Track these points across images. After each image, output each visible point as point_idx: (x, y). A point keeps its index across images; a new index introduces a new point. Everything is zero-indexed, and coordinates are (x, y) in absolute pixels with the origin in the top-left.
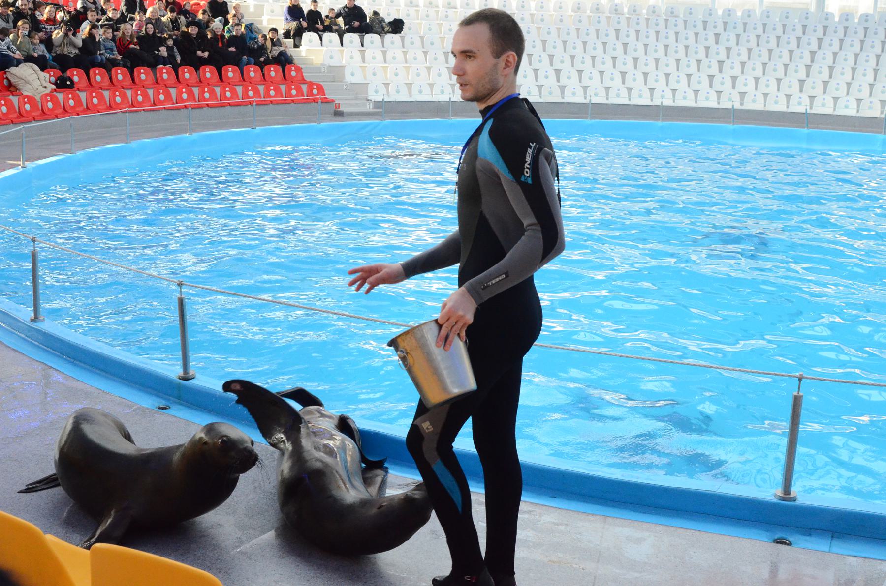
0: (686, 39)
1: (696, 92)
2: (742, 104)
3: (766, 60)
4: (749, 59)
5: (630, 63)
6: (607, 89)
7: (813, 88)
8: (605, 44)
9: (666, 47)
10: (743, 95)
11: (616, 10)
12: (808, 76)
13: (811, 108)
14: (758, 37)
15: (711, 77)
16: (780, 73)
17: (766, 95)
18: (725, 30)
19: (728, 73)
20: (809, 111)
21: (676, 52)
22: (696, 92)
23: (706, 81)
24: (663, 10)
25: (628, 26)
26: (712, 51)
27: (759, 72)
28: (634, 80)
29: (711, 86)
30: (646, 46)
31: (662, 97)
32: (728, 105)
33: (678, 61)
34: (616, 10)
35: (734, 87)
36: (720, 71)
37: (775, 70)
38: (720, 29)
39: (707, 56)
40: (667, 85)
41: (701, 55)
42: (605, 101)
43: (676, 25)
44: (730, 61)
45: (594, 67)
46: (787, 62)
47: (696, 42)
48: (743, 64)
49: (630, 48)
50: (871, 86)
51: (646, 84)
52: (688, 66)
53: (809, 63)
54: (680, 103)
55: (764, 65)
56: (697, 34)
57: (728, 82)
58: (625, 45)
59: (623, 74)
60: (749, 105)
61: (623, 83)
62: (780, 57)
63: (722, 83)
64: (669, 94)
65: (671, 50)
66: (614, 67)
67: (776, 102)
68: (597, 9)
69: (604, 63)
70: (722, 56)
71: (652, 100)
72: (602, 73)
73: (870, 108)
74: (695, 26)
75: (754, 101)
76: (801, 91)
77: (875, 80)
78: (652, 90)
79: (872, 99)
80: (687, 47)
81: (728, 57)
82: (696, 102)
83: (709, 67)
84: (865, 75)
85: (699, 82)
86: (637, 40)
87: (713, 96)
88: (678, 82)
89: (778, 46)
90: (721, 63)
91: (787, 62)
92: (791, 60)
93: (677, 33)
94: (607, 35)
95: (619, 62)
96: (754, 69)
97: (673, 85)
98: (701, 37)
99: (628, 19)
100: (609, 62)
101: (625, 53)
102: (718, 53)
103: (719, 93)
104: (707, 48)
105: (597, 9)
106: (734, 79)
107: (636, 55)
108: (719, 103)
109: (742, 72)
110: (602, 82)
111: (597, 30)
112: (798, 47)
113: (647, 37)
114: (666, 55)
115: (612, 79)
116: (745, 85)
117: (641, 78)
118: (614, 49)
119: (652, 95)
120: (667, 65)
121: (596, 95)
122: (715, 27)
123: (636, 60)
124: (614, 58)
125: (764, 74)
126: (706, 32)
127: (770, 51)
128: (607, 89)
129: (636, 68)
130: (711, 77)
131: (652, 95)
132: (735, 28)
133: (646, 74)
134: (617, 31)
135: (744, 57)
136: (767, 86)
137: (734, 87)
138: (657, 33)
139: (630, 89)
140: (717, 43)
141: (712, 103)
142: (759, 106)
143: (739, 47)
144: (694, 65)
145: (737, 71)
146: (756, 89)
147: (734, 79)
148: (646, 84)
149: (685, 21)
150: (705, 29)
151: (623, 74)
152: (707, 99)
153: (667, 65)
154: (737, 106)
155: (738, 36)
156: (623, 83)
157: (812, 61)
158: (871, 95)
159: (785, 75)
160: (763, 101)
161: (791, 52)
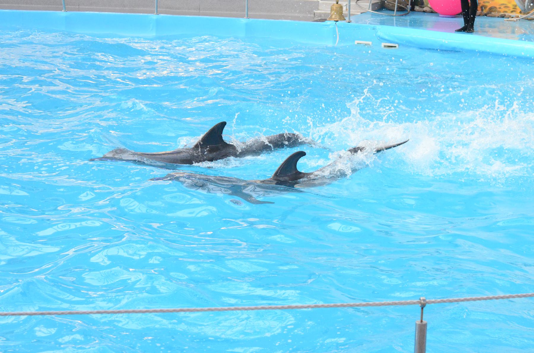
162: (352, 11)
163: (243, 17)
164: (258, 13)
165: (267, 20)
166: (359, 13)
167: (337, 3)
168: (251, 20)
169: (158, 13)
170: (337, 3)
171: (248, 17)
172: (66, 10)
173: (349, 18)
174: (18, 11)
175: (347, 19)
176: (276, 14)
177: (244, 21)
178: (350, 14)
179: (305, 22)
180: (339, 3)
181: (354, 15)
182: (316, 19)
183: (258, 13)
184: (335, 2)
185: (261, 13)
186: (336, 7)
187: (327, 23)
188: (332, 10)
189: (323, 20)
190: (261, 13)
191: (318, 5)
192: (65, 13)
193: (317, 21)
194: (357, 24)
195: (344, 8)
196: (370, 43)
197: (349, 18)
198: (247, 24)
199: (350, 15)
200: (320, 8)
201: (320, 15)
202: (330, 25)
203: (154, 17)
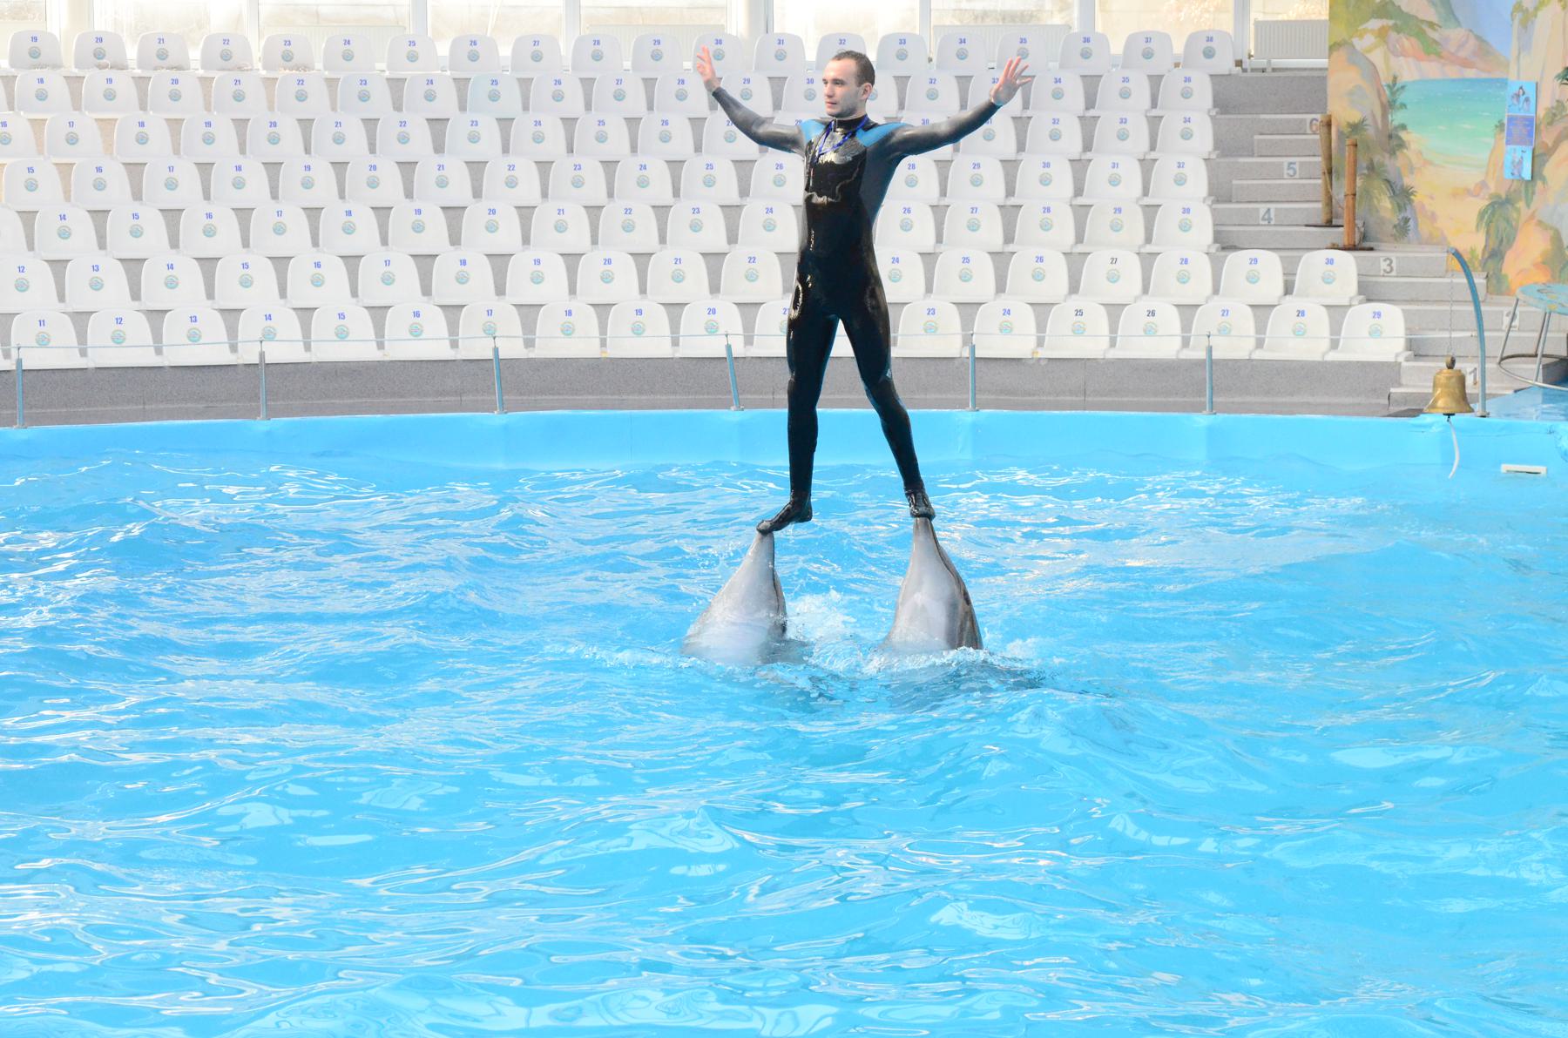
0: (339, 140)
1: (378, 313)
2: (529, 343)
3: (600, 196)
4: (545, 195)
5: (156, 229)
6: (80, 319)
7: (751, 277)
8: (65, 169)
9: (273, 168)
10: (528, 312)
11: (99, 55)
12: (732, 239)
13: (749, 341)
14: (569, 123)
15: (425, 262)
16: (646, 236)
17: (602, 309)
18: (463, 108)
19: (479, 241)
20: (739, 350)
21: (307, 184)
22: (378, 313)
23: (408, 274)
24: (257, 53)
25: (143, 107)
26: (425, 175)
27: (577, 237)
28: (171, 284)
29: (426, 291)
30: (205, 168)
31: (269, 335)
32: (479, 349)
33: (313, 213)
34: (99, 55)
35: (500, 291)
36: (455, 240)
37: (628, 228)
38: (446, 104)
39: (409, 194)
40: (283, 293)
41: (390, 188)
42: (77, 362)
43: (301, 97)
44: (484, 205)
45: (31, 246)
46: (666, 197)
47: (372, 150)
48: (525, 213)
49: (153, 179)
50: (929, 258)
51: (210, 295)
52: (349, 229)
53: (734, 198)
54: (328, 351)
55: (594, 211)
56: (370, 124)
57: (482, 273)
58: (135, 170)
59: (133, 266)
60: (553, 345)
61: (136, 296)
62: (643, 183)
63: (462, 279)
64: (289, 326)
65: (290, 178)
66: (102, 245)
67: (638, 331)
68: (34, 54)
69: (64, 234)
70: (459, 191)
71: (234, 348)
72: (58, 266)
73: (930, 329)
74: (364, 97)
75: (568, 331)
76: (715, 288)
77: (939, 240)
78: (231, 315)
79: (932, 301)
80: (340, 167)
81: (477, 193)
82: (381, 346)
83: (418, 228)
84: (906, 226)
85: (388, 280)
86: (176, 151)
87: (436, 322)
88: (317, 282)
89: (634, 149)
90: (453, 213)
91: (666, 197)
92: (676, 193)
93: (306, 124)
94: (72, 140)
95: (117, 227)
96: (560, 228)
97: (302, 293)
98: (387, 132)
99: (141, 82)
100: (83, 228)
101: (137, 195)
102: (442, 183)
103: (452, 311)
104: (407, 168)
105: (34, 54)
106: (499, 262)
107: (171, 200)
108: (454, 344)
109: (526, 240)
110: (61, 298)
111: (37, 124)
112: (698, 149)
113: (209, 140)
114: (275, 196)
115: (96, 285)
116: (537, 279)
117: (191, 277)
118: (100, 186)
119: (232, 331)
120: (279, 230)
121: (43, 342)
122: (430, 97)
123: (172, 216)
124: (99, 216)
125: (595, 241)
126: (404, 116)
127: (610, 166)
128: (80, 319)
129: (174, 243)
130: (425, 262)
131: (232, 331)
132: (494, 97)
133: (208, 264)
134: (106, 125)
135: (528, 190)
136: (607, 278)
137: (500, 291)
138: (241, 124)
139: (156, 316)
140: (439, 148)
141: (433, 347)
142: (583, 345)
143: (511, 159)
144: (367, 224)
145: (507, 237)
146: (572, 291)
147: (499, 262)
148: (210, 295)
149: (331, 83)
150: (398, 107)
151: (133, 266)
152: (416, 332)
153: (279, 230)
154: (512, 348)
155: (505, 123)
156: (136, 296)
157: (744, 192)
158: (929, 290)
159: (663, 240)
160: (595, 332)
161: (675, 166)
162: (1491, 387)
163: (1197, 408)
164: (1238, 399)
165: (1264, 416)
166: (1510, 392)
167: (1451, 365)
168: (1221, 417)
169: (977, 406)
170: (1451, 365)
171: (1213, 410)
172: (742, 406)
173: (1484, 407)
174: (619, 412)
175: (1477, 407)
176: (1287, 399)
177: (1202, 420)
178: (1485, 396)
179: (1367, 419)
180: (1457, 366)
181: (1494, 396)
182: (1394, 409)
183: (1238, 399)
184: (1444, 365)
185: (1248, 399)
186: (1449, 378)
187: (1425, 419)
188: (1435, 386)
189: (1415, 413)
190: (1248, 399)
191: (1399, 373)
192: (738, 413)
193: (1396, 415)
194: (1506, 421)
195: (1469, 381)
196: (1542, 469)
197: (1484, 407)
198: (1211, 430)
199: (1485, 396)
200: (1404, 381)
201: (1406, 398)
202: (1430, 426)
203: (966, 416)
